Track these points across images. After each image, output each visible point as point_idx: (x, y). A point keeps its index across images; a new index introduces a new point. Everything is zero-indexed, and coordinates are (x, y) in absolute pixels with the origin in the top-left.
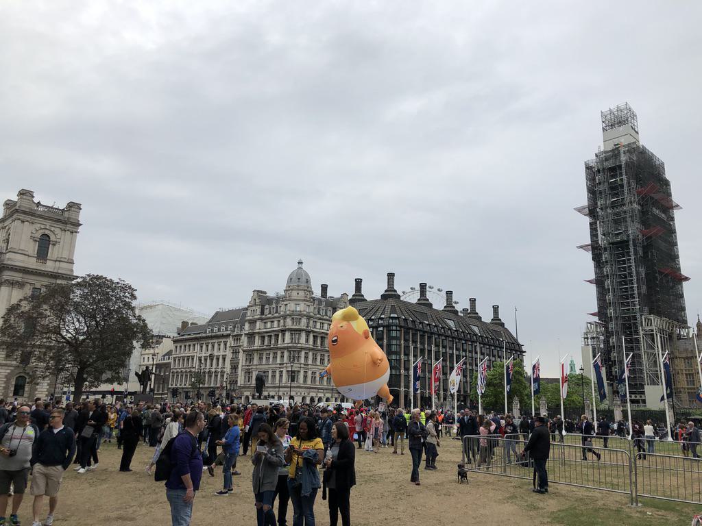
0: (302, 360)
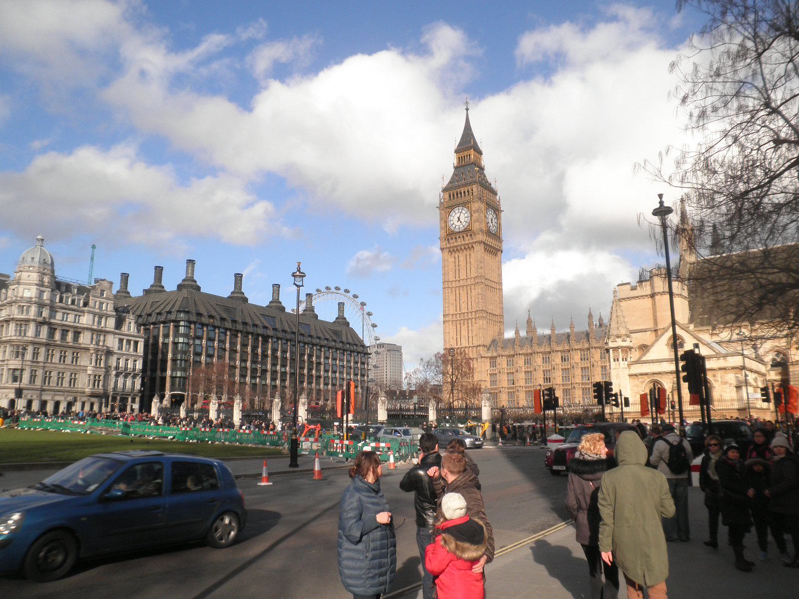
0: (29, 356)
